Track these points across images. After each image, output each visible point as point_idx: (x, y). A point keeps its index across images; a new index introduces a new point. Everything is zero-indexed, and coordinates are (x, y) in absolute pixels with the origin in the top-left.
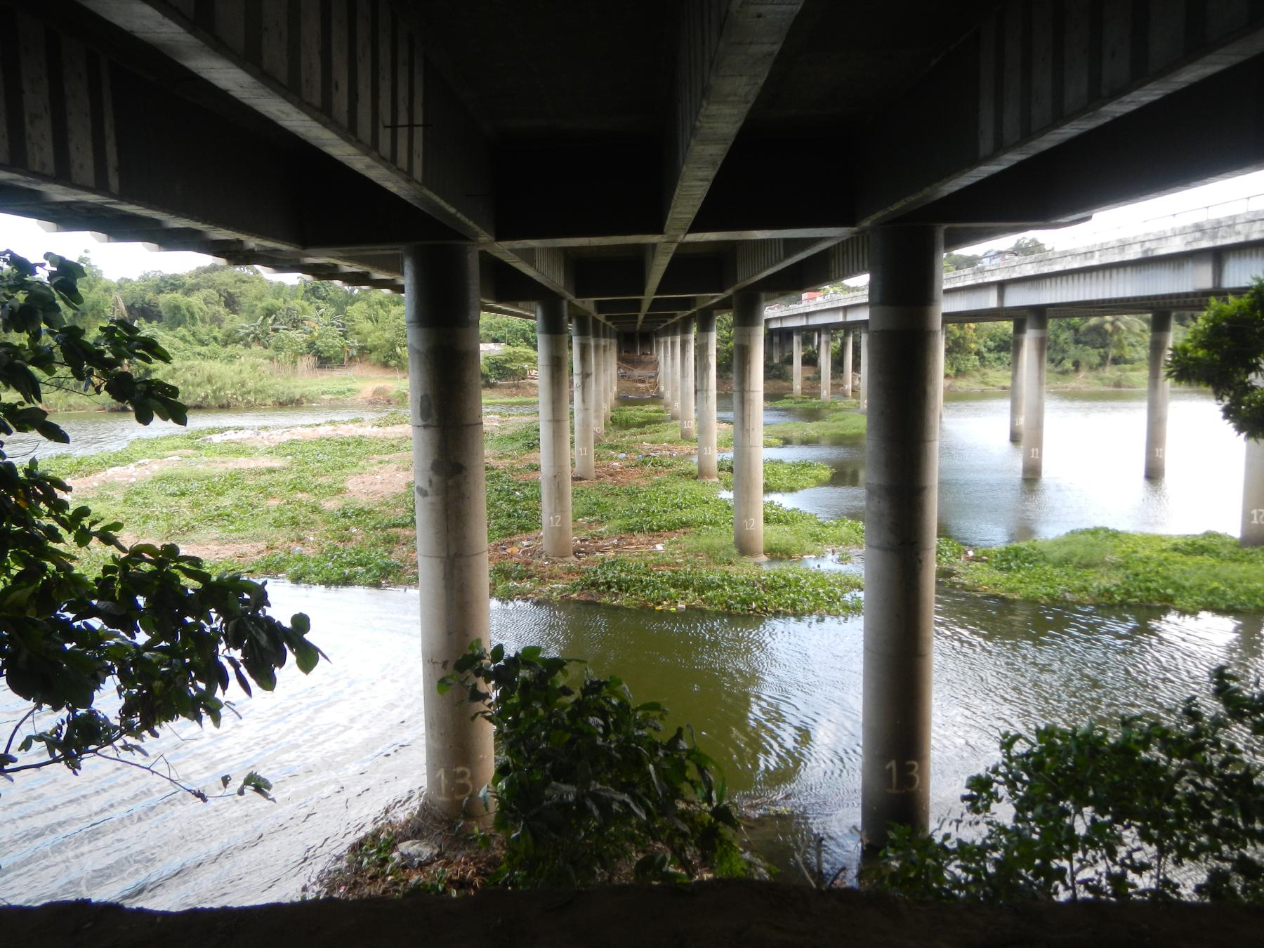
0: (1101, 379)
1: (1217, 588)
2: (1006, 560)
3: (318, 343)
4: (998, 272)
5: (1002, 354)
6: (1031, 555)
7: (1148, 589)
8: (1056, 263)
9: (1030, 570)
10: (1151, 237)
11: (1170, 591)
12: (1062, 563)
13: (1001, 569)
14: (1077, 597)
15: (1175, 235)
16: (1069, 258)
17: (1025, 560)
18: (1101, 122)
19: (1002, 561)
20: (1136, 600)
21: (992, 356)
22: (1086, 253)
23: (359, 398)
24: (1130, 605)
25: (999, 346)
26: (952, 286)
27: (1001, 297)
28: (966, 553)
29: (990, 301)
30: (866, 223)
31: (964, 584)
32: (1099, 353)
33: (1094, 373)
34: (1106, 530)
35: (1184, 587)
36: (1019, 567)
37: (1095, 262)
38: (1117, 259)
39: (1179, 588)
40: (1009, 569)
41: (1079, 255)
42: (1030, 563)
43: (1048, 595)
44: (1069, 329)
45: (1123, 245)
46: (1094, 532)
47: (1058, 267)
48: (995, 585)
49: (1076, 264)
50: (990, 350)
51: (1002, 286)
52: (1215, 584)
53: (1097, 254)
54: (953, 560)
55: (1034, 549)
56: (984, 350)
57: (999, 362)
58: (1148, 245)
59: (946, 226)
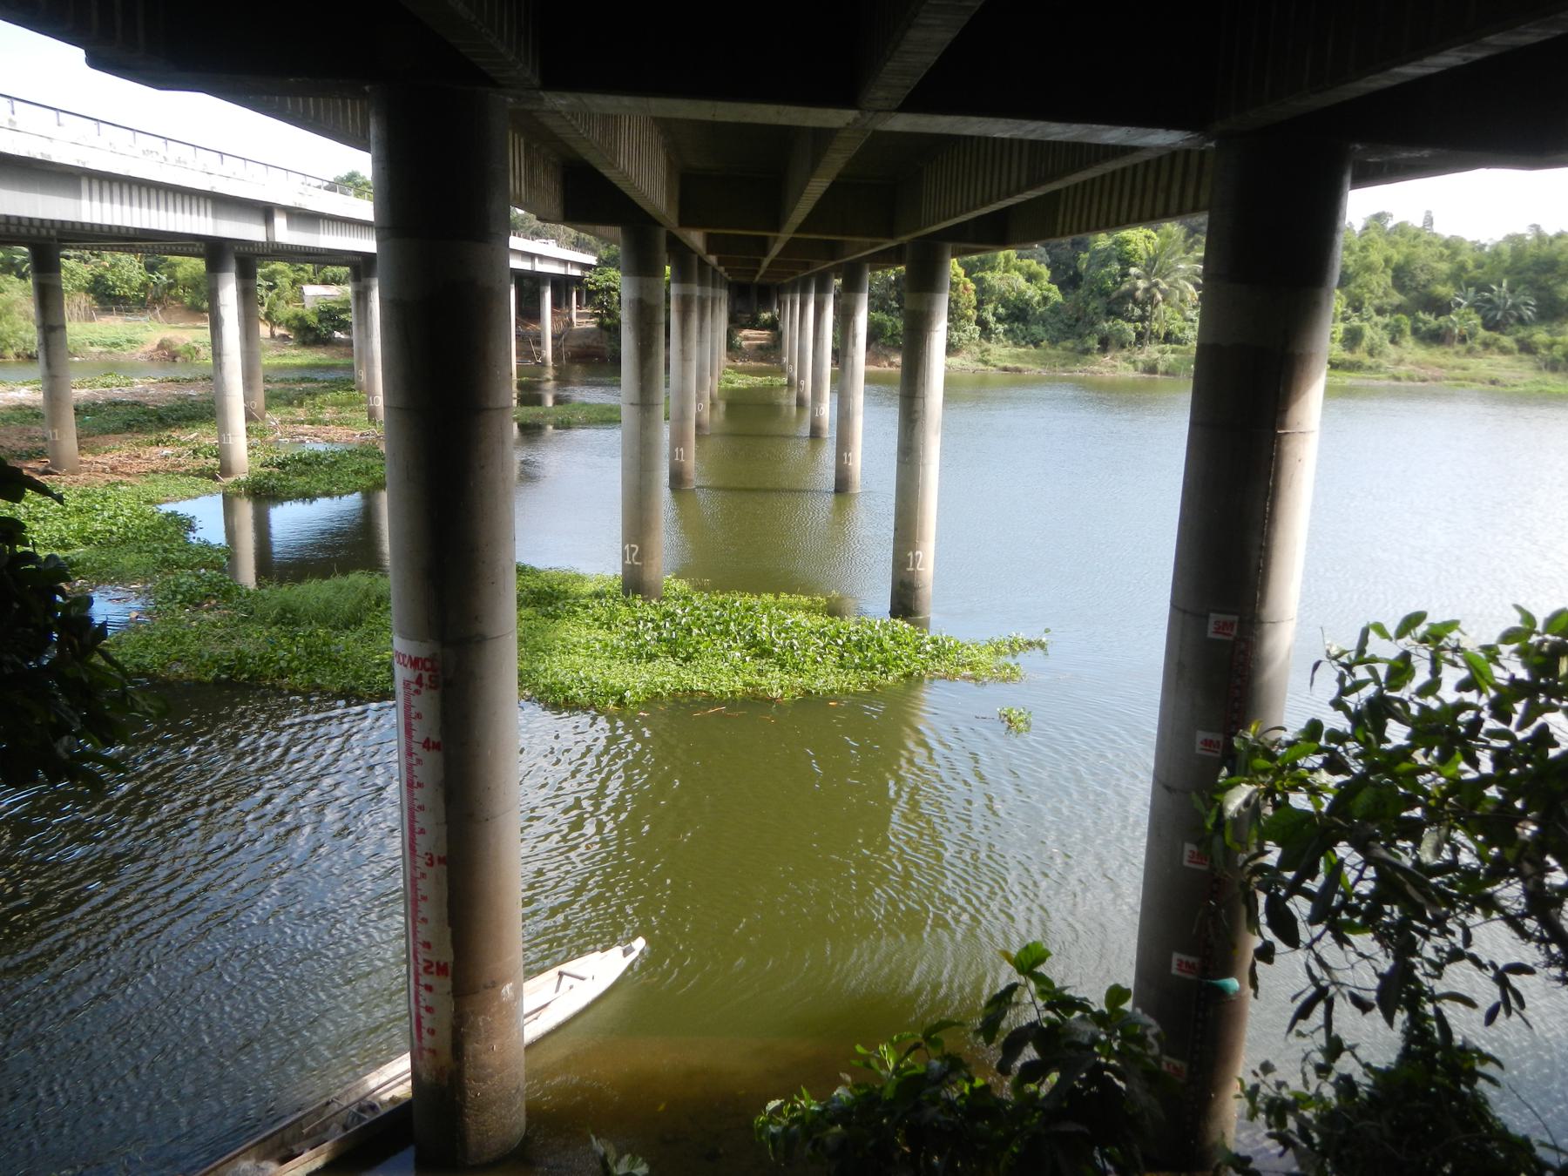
0: (1134, 363)
3: (109, 276)
21: (1001, 328)
23: (139, 353)
25: (1012, 314)
32: (1136, 328)
33: (1125, 353)
44: (1101, 295)
50: (1000, 320)
56: (991, 319)
57: (1010, 335)
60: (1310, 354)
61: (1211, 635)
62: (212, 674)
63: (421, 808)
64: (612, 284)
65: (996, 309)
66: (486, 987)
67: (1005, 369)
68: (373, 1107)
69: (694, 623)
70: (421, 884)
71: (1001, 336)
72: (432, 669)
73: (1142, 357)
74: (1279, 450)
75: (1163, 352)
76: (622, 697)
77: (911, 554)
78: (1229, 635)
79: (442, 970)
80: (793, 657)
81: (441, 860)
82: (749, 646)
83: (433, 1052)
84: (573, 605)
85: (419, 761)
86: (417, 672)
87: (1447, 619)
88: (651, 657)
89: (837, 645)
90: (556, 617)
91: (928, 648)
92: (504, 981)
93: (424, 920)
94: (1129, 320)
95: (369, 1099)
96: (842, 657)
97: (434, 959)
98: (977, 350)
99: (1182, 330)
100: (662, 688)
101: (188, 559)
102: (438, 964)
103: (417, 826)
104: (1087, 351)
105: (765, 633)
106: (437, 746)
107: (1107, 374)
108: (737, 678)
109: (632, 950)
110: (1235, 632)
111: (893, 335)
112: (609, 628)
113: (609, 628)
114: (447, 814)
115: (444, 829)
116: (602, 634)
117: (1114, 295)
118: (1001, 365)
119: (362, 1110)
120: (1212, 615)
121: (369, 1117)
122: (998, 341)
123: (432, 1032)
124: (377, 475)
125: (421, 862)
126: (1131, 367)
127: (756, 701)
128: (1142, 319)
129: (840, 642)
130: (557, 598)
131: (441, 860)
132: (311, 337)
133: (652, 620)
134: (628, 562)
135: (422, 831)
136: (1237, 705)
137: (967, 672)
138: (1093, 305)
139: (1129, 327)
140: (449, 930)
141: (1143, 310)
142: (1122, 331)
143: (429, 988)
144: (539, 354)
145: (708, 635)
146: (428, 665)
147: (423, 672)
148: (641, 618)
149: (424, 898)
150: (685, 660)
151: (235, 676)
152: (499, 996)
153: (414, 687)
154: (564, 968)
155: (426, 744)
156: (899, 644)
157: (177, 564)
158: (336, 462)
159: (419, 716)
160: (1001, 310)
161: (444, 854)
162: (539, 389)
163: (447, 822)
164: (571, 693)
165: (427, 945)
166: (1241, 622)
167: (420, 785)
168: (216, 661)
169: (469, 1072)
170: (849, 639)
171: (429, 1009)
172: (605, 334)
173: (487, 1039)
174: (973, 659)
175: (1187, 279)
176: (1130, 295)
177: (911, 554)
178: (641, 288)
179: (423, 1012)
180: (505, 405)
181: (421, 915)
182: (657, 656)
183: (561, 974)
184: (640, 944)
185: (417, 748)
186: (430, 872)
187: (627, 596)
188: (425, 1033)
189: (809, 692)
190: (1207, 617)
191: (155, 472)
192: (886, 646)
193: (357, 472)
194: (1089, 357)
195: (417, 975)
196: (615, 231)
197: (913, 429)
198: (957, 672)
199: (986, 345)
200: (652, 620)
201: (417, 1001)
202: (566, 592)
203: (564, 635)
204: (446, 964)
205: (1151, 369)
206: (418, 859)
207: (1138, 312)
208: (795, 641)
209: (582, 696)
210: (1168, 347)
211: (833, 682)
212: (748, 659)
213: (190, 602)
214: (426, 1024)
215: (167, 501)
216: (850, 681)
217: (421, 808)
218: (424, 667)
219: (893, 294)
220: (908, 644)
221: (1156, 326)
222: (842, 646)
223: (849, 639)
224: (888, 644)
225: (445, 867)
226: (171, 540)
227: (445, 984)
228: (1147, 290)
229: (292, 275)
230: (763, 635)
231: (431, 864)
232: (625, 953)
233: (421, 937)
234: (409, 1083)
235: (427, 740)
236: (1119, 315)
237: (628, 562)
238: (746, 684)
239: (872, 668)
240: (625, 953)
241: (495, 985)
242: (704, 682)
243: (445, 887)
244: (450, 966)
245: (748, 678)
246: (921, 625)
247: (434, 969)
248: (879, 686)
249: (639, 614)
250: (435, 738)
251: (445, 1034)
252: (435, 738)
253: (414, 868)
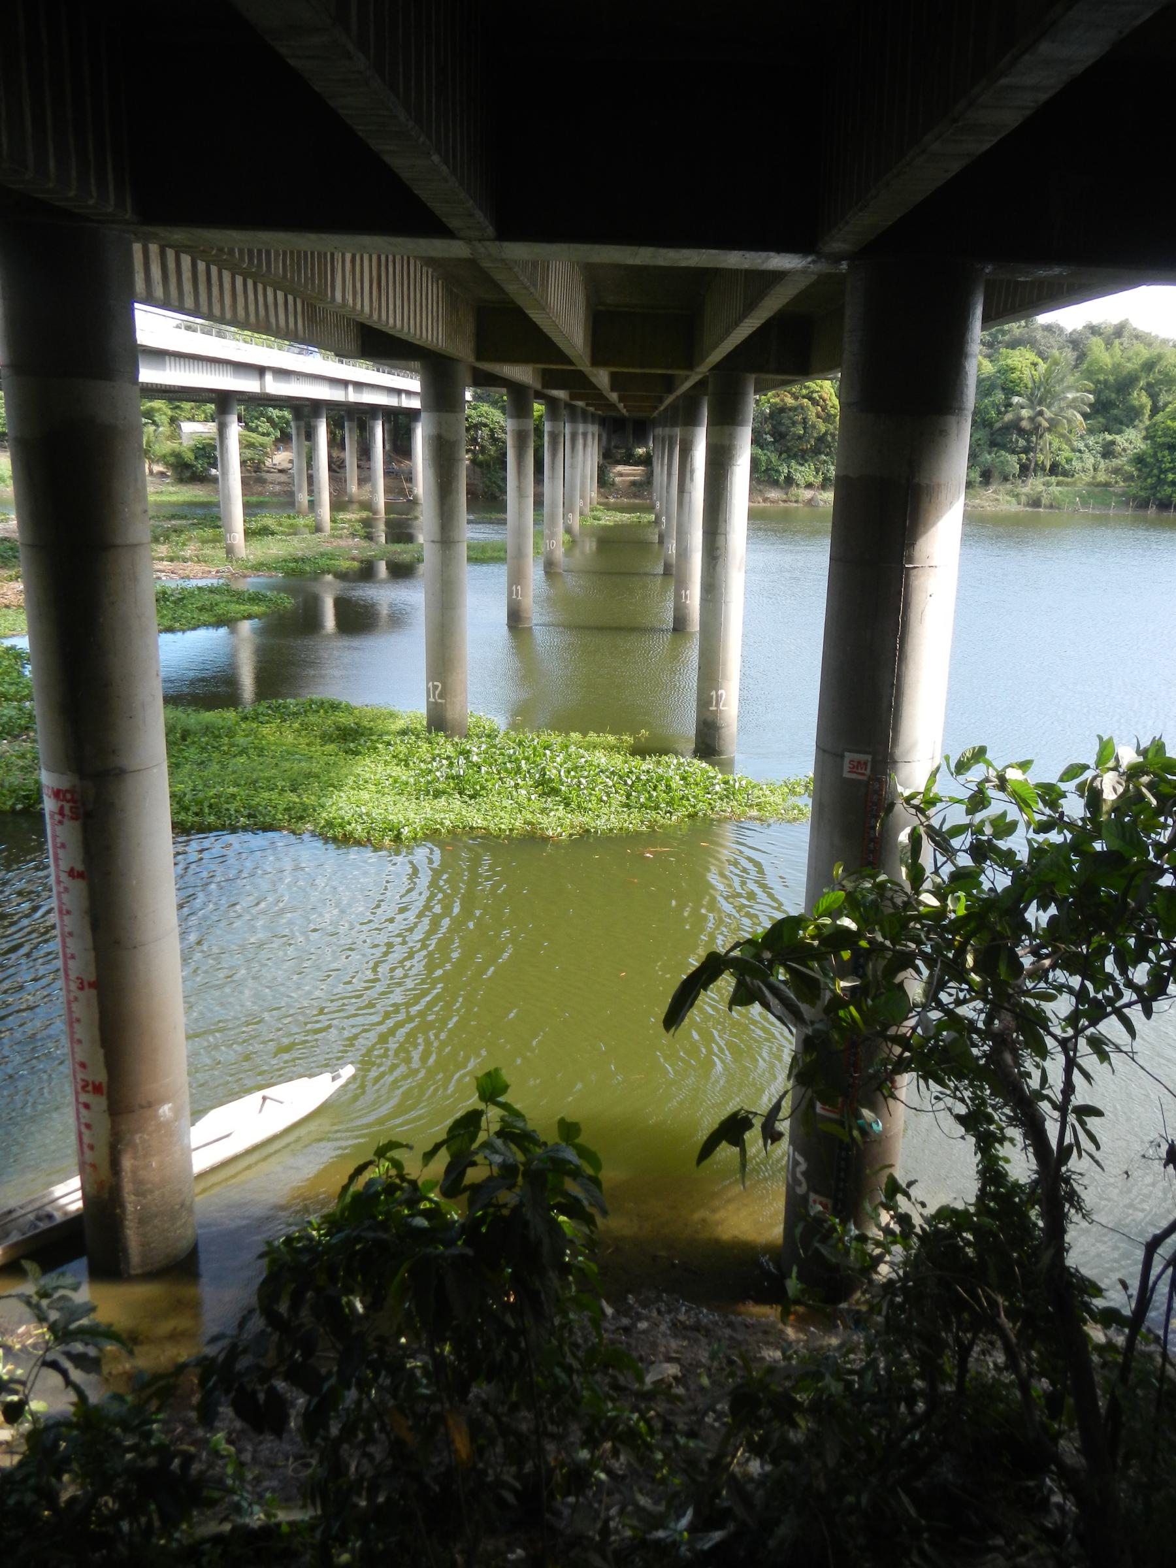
0: (1017, 496)
32: (1020, 460)
33: (1009, 486)
60: (939, 485)
61: (846, 775)
62: (10, 803)
63: (71, 934)
64: (484, 420)
66: (142, 1107)
68: (50, 1217)
69: (484, 761)
70: (74, 1006)
72: (72, 800)
73: (1026, 490)
74: (907, 586)
76: (400, 833)
77: (714, 693)
78: (863, 774)
79: (97, 1089)
80: (578, 796)
81: (91, 985)
82: (538, 784)
83: (93, 1166)
84: (377, 741)
85: (66, 889)
86: (60, 803)
87: (1082, 762)
88: (437, 794)
89: (626, 784)
90: (356, 753)
91: (717, 788)
92: (162, 1102)
93: (79, 1041)
94: (1013, 452)
95: (49, 1209)
96: (628, 796)
97: (90, 1079)
99: (1069, 461)
100: (442, 824)
101: (17, 692)
102: (93, 1083)
103: (69, 951)
105: (554, 771)
106: (81, 875)
108: (519, 816)
109: (339, 1076)
110: (868, 772)
111: (767, 470)
112: (407, 765)
113: (407, 765)
114: (94, 940)
115: (92, 954)
116: (397, 771)
117: (998, 425)
119: (39, 1218)
120: (847, 754)
121: (43, 1225)
123: (91, 1147)
124: (221, 612)
125: (73, 986)
126: (1014, 500)
127: (533, 839)
128: (1026, 450)
129: (629, 782)
130: (362, 735)
131: (91, 985)
132: (188, 474)
133: (448, 758)
134: (432, 699)
135: (73, 957)
136: (872, 845)
137: (754, 813)
139: (1013, 459)
140: (101, 1052)
141: (1028, 441)
143: (87, 1106)
144: (411, 491)
145: (499, 773)
146: (68, 796)
147: (64, 803)
148: (439, 755)
149: (78, 1020)
150: (472, 797)
151: (30, 806)
152: (156, 1116)
153: (57, 817)
154: (266, 1092)
155: (71, 873)
156: (687, 784)
157: (5, 696)
158: (183, 598)
159: (63, 846)
161: (93, 978)
162: (409, 526)
163: (96, 948)
164: (348, 828)
165: (83, 1065)
166: (874, 761)
167: (68, 912)
168: (14, 791)
169: (128, 1187)
170: (638, 778)
171: (88, 1126)
172: (478, 470)
173: (145, 1156)
174: (763, 799)
175: (1075, 408)
176: (1015, 426)
177: (714, 693)
178: (439, 424)
179: (83, 1129)
180: (135, 542)
181: (77, 1036)
182: (444, 793)
183: (264, 1098)
184: (348, 1071)
185: (64, 877)
186: (79, 994)
187: (430, 733)
188: (86, 1149)
189: (588, 831)
190: (843, 756)
191: (7, 607)
192: (674, 786)
193: (201, 609)
195: (77, 1093)
196: (417, 364)
197: (714, 568)
198: (744, 812)
200: (448, 758)
201: (78, 1118)
202: (371, 729)
203: (359, 770)
204: (100, 1084)
205: (1036, 503)
206: (71, 983)
207: (1022, 443)
208: (583, 781)
209: (359, 830)
210: (1053, 479)
211: (614, 822)
212: (533, 797)
213: (8, 734)
214: (86, 1140)
215: (14, 635)
216: (634, 821)
217: (71, 934)
218: (64, 799)
219: (768, 427)
220: (697, 784)
221: (1041, 457)
222: (631, 787)
223: (638, 778)
224: (676, 783)
225: (94, 992)
226: (7, 673)
227: (100, 1103)
228: (1032, 419)
229: (170, 413)
230: (552, 773)
231: (81, 988)
232: (334, 1079)
233: (80, 1057)
234: (79, 1194)
235: (72, 870)
236: (1003, 447)
237: (432, 699)
238: (526, 823)
239: (657, 808)
240: (334, 1079)
241: (151, 1105)
242: (485, 819)
243: (95, 1010)
244: (105, 1086)
245: (529, 816)
246: (726, 766)
247: (90, 1088)
248: (659, 827)
249: (437, 752)
250: (79, 867)
251: (103, 1151)
252: (79, 867)
253: (69, 991)
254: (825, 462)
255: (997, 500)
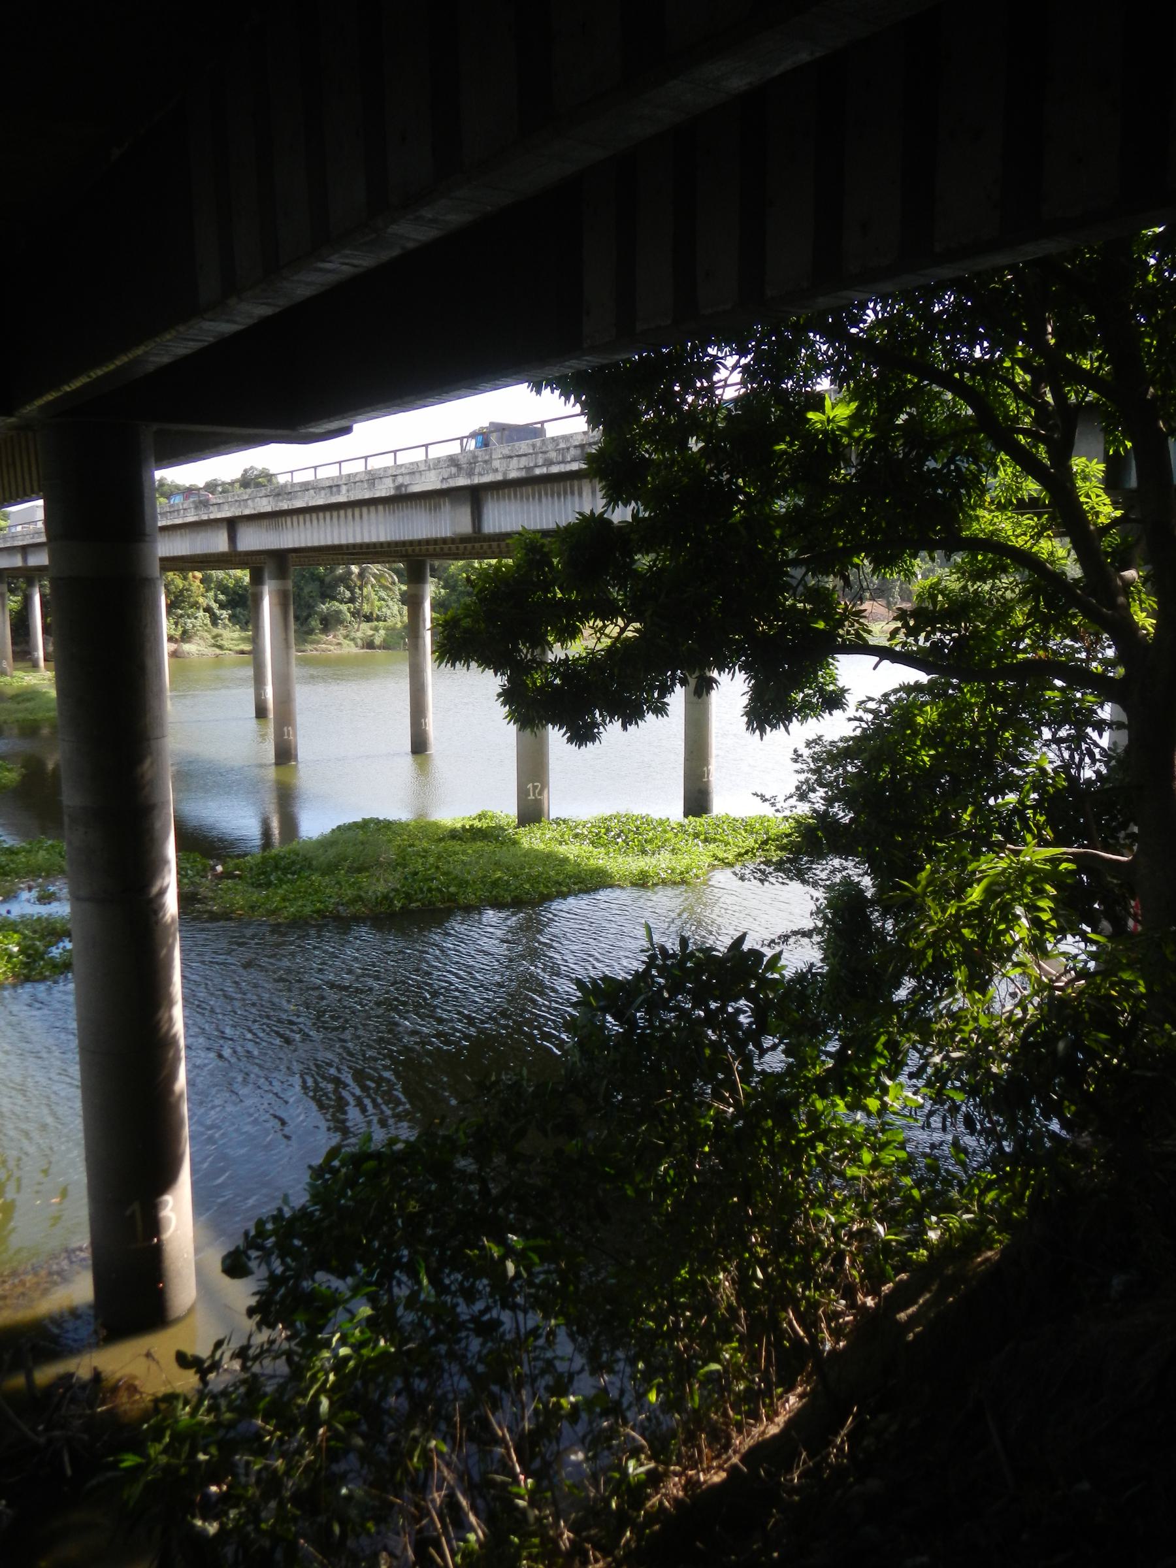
0: (353, 639)
1: (500, 878)
2: (264, 873)
4: (226, 507)
5: (238, 610)
6: (293, 863)
7: (430, 890)
8: (296, 498)
9: (292, 882)
10: (403, 470)
11: (452, 889)
12: (330, 869)
13: (260, 886)
14: (352, 909)
15: (429, 469)
16: (312, 492)
17: (285, 870)
18: (385, 256)
19: (260, 874)
20: (419, 904)
21: (225, 614)
22: (331, 487)
24: (412, 912)
25: (233, 600)
26: (169, 523)
27: (232, 539)
28: (213, 868)
29: (219, 543)
30: (32, 408)
31: (211, 912)
33: (342, 631)
34: (377, 822)
35: (467, 882)
36: (280, 880)
37: (342, 498)
38: (367, 496)
39: (463, 884)
40: (269, 884)
41: (323, 488)
42: (293, 873)
43: (318, 912)
44: (314, 580)
45: (373, 478)
46: (365, 824)
47: (299, 504)
48: (252, 908)
49: (320, 502)
50: (222, 606)
51: (232, 525)
52: (499, 874)
53: (344, 489)
54: (197, 879)
55: (298, 855)
56: (215, 606)
58: (400, 480)
59: (155, 427)
65: (216, 596)
67: (242, 652)
71: (227, 621)
73: (359, 634)
75: (376, 629)
94: (341, 602)
98: (206, 635)
104: (311, 632)
107: (335, 651)
118: (237, 648)
122: (225, 626)
126: (352, 644)
128: (352, 600)
138: (306, 590)
139: (344, 607)
141: (353, 592)
142: (339, 612)
160: (221, 597)
194: (313, 637)
199: (215, 631)
207: (348, 594)
236: (333, 598)
254: (182, 616)
255: (339, 644)
